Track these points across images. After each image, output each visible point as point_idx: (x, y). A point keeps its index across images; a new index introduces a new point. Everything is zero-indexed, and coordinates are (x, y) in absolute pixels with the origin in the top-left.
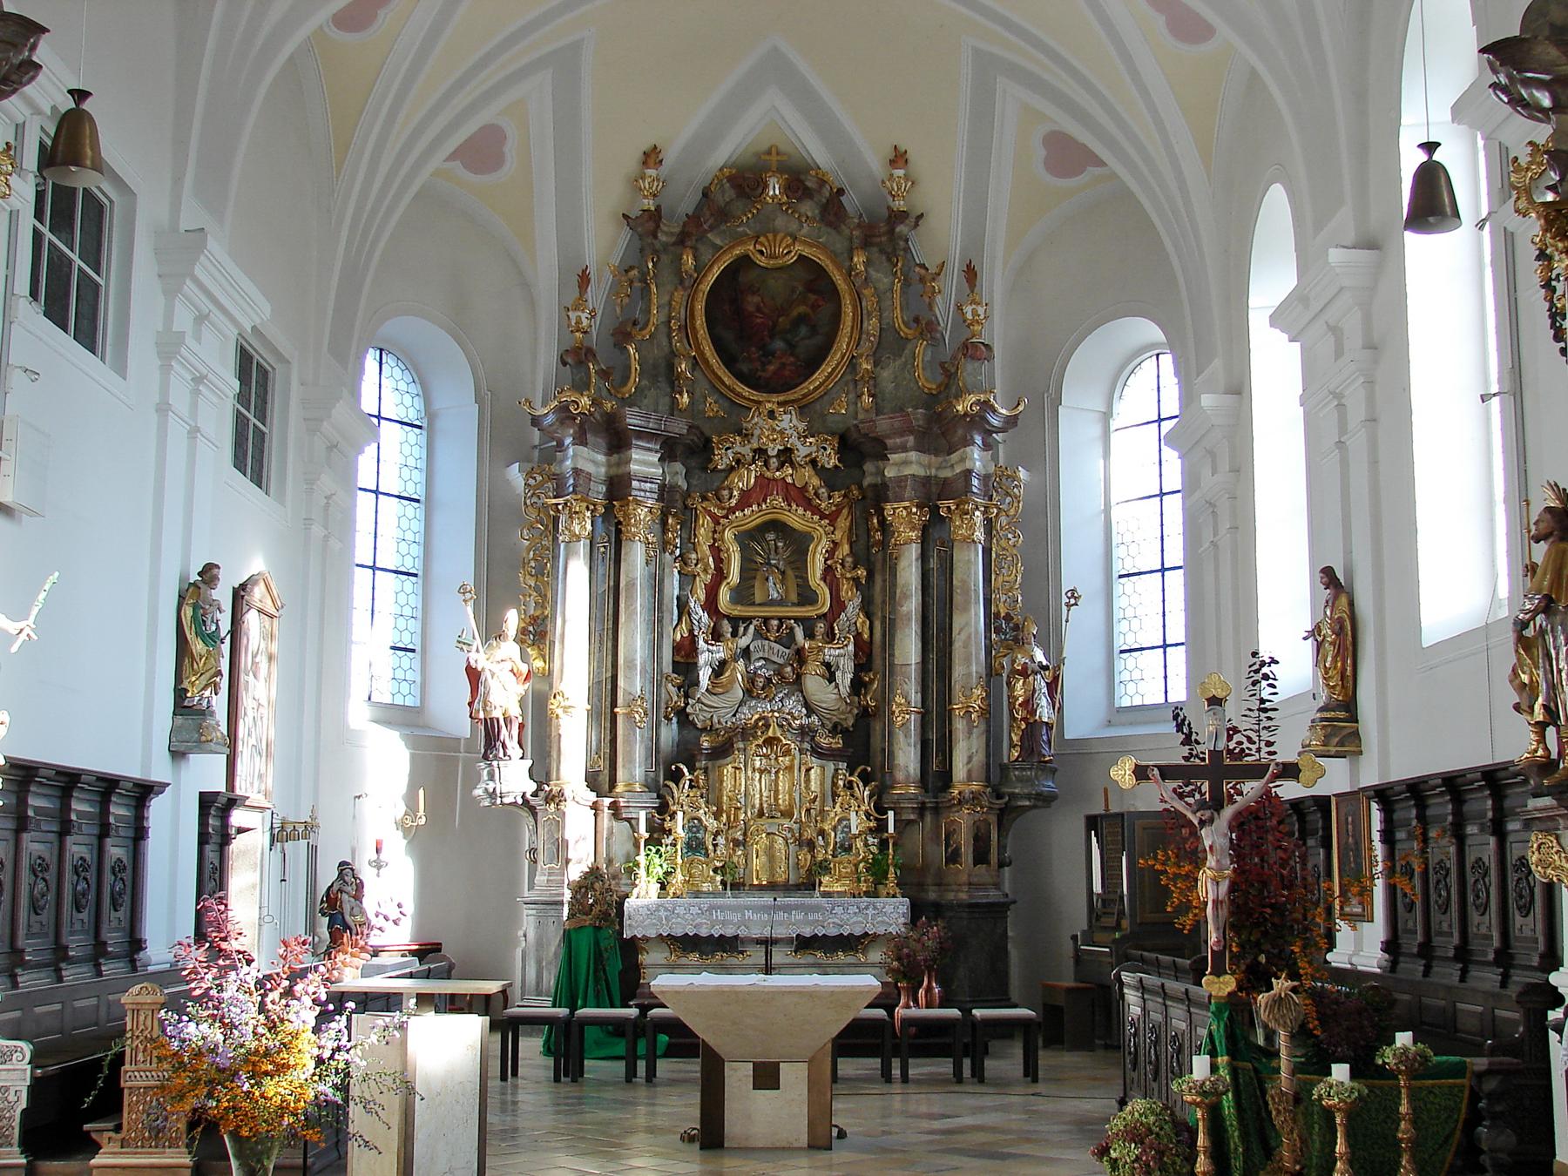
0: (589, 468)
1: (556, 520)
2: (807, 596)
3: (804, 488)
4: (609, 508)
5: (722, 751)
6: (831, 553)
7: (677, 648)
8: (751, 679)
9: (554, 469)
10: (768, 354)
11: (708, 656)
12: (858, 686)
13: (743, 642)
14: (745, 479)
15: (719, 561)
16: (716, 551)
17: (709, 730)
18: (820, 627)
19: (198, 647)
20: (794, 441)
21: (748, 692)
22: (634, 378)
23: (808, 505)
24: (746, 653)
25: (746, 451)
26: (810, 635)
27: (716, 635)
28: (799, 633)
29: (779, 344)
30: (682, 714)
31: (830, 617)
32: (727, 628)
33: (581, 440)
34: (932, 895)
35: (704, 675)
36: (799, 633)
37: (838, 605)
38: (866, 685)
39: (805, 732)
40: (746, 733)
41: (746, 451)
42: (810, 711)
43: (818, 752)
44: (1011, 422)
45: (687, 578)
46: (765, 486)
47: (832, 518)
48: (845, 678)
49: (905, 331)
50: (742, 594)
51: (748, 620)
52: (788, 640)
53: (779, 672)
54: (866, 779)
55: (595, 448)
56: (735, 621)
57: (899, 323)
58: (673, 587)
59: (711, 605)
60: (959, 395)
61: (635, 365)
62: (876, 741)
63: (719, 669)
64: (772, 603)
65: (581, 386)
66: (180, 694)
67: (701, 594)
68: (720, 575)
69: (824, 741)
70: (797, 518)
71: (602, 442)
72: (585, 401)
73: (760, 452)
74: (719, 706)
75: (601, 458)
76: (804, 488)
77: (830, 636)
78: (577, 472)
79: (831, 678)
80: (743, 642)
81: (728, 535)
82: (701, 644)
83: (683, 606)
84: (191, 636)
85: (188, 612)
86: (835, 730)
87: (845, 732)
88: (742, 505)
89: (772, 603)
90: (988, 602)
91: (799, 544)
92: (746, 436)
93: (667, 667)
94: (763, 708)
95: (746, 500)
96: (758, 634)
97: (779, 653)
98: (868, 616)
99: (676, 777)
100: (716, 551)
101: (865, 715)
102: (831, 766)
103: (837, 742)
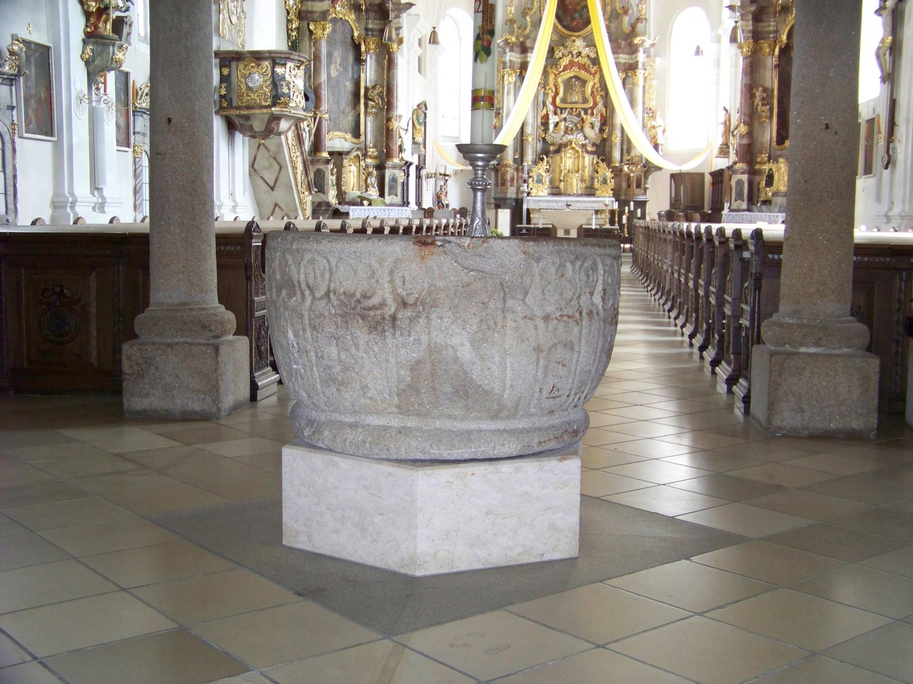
0: (514, 59)
1: (503, 77)
2: (585, 101)
3: (584, 65)
4: (521, 72)
5: (558, 151)
6: (593, 87)
7: (542, 118)
8: (567, 128)
9: (503, 59)
10: (573, 19)
11: (553, 119)
12: (602, 131)
13: (564, 116)
14: (565, 62)
15: (556, 89)
16: (556, 86)
17: (553, 144)
18: (589, 111)
19: (418, 127)
20: (581, 49)
21: (566, 132)
22: (529, 28)
23: (587, 70)
24: (565, 119)
25: (566, 52)
26: (586, 113)
27: (555, 113)
28: (582, 113)
29: (577, 15)
30: (544, 139)
31: (592, 108)
32: (559, 111)
33: (512, 50)
34: (623, 198)
35: (551, 127)
36: (582, 113)
37: (595, 104)
38: (604, 131)
39: (584, 146)
40: (566, 145)
41: (566, 52)
42: (586, 138)
43: (587, 152)
44: (653, 45)
45: (546, 95)
46: (571, 64)
47: (594, 74)
48: (597, 128)
49: (620, 11)
50: (564, 100)
51: (566, 109)
52: (579, 115)
53: (576, 125)
54: (603, 161)
55: (517, 52)
56: (562, 109)
57: (618, 8)
58: (541, 98)
59: (554, 103)
60: (636, 36)
61: (529, 24)
62: (607, 149)
63: (556, 125)
64: (573, 103)
65: (512, 33)
66: (414, 139)
67: (550, 99)
68: (557, 94)
69: (589, 149)
70: (583, 74)
71: (518, 50)
72: (514, 39)
73: (571, 53)
74: (555, 136)
75: (518, 55)
76: (584, 65)
77: (592, 114)
78: (510, 61)
79: (593, 128)
80: (564, 116)
81: (560, 80)
82: (550, 117)
83: (544, 104)
84: (416, 123)
85: (415, 116)
86: (594, 144)
87: (597, 145)
88: (564, 70)
89: (573, 103)
90: (644, 103)
91: (584, 82)
92: (566, 47)
93: (539, 124)
94: (570, 137)
95: (565, 69)
96: (569, 113)
97: (576, 120)
98: (606, 107)
99: (542, 159)
100: (556, 86)
101: (604, 140)
102: (592, 156)
103: (594, 149)
